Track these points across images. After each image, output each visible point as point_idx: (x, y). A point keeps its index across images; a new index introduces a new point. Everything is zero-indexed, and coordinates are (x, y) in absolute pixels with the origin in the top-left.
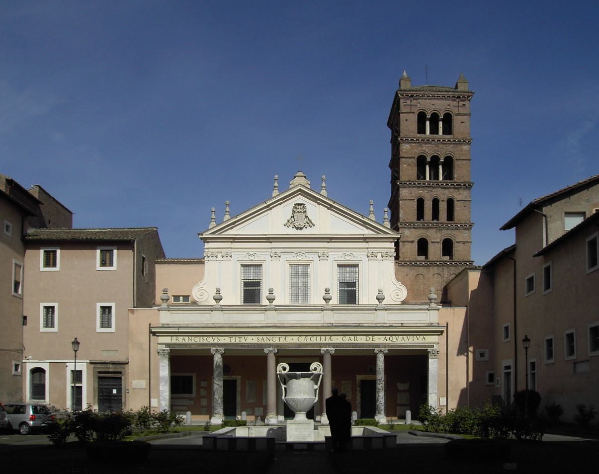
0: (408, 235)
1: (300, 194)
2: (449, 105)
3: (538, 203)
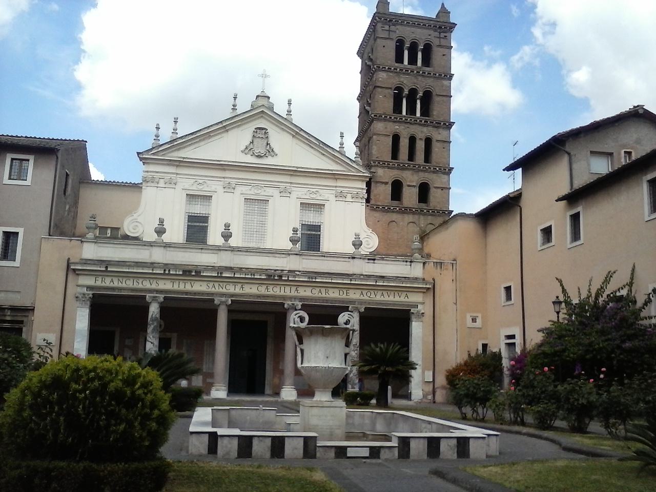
0: (382, 175)
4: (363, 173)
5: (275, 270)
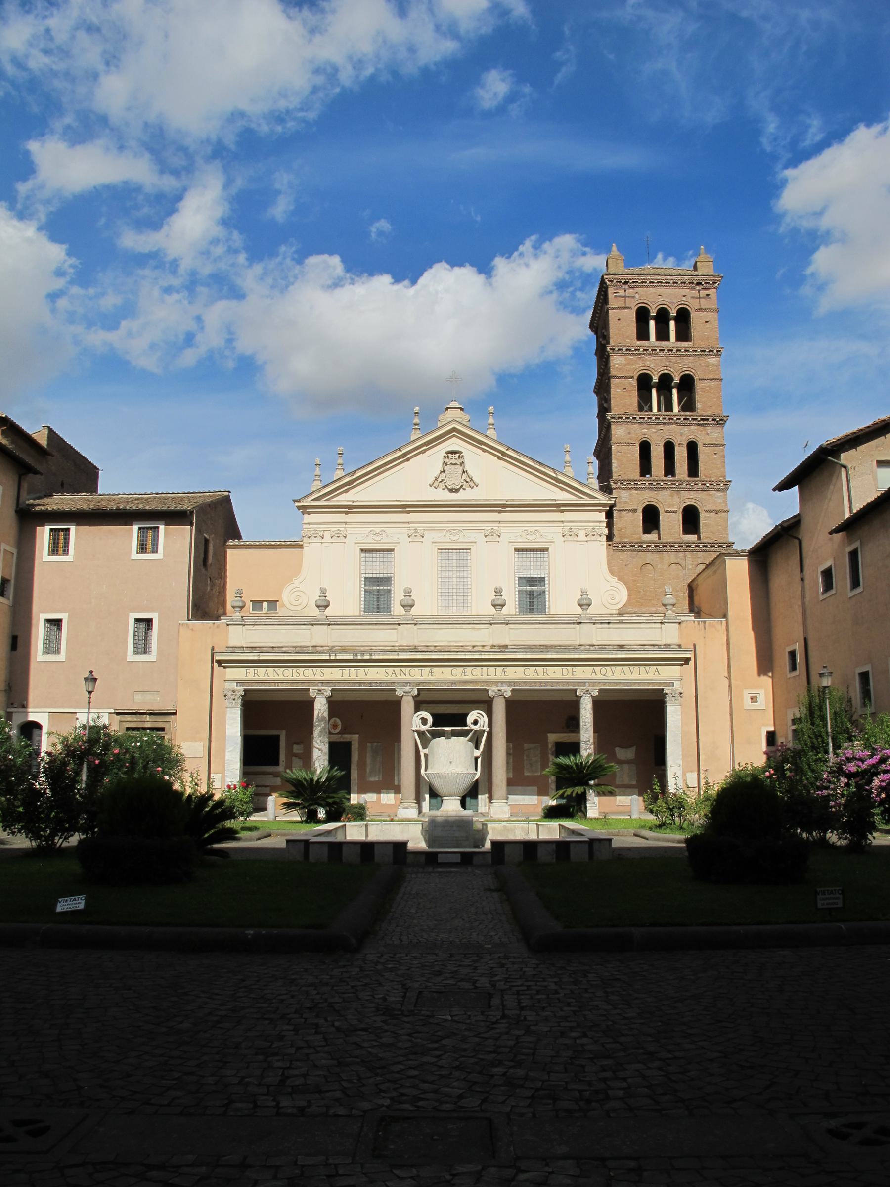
0: (627, 499)
1: (454, 436)
2: (684, 296)
3: (834, 446)
4: (600, 500)
5: (474, 647)
